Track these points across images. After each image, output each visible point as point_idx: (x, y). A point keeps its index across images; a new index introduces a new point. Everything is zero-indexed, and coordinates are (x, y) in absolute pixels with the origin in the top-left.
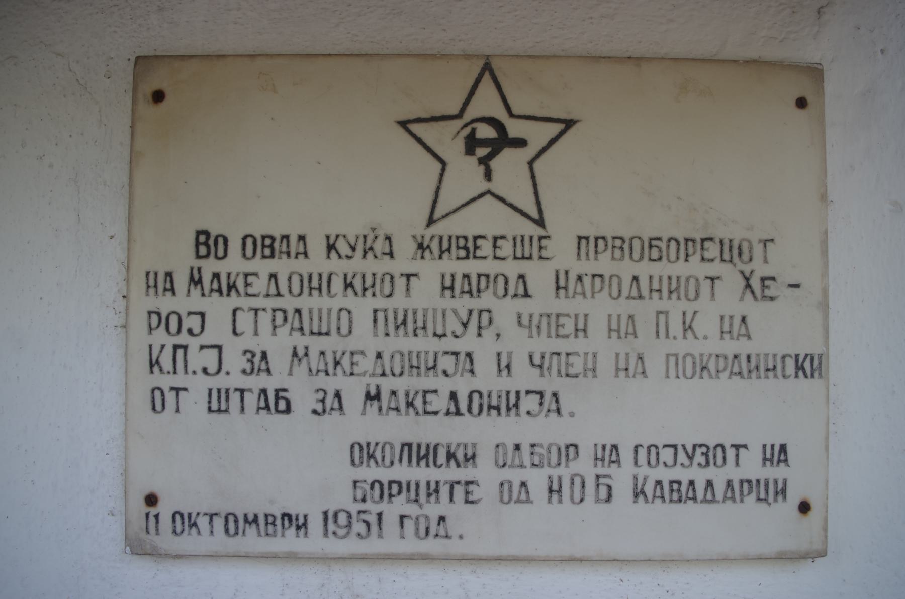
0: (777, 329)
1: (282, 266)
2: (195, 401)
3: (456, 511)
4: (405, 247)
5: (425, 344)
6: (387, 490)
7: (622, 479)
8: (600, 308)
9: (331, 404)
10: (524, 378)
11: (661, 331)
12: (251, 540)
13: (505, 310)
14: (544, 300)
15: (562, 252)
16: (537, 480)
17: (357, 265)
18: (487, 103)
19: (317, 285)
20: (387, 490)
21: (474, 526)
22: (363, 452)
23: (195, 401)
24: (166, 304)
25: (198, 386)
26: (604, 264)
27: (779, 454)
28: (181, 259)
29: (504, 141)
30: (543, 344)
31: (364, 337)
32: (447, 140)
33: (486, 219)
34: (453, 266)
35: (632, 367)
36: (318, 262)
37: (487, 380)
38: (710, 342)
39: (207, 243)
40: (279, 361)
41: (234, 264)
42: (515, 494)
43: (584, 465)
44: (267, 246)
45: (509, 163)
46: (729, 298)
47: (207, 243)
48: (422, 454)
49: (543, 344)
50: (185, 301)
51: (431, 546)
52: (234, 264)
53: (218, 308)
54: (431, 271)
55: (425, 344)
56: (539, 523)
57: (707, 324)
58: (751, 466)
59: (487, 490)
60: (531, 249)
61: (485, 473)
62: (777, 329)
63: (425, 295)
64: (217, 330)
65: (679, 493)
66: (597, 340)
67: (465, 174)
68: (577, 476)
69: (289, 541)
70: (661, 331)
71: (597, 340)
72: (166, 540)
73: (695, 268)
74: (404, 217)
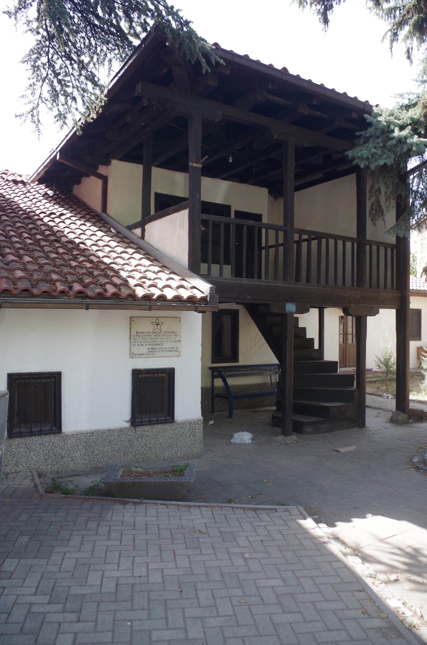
0: (177, 338)
1: (143, 334)
2: (136, 345)
3: (155, 353)
4: (151, 333)
5: (153, 340)
6: (150, 352)
7: (166, 350)
8: (165, 337)
9: (146, 345)
10: (160, 343)
11: (169, 339)
12: (141, 356)
13: (158, 337)
14: (161, 337)
15: (162, 332)
16: (161, 350)
17: (148, 334)
18: (157, 321)
19: (145, 336)
20: (150, 352)
21: (157, 354)
22: (149, 349)
23: (136, 345)
24: (134, 337)
25: (137, 344)
26: (165, 334)
27: (177, 348)
28: (135, 334)
29: (158, 324)
30: (161, 340)
31: (149, 340)
32: (154, 324)
33: (157, 330)
34: (155, 334)
35: (167, 342)
36: (145, 334)
37: (157, 343)
38: (173, 340)
39: (137, 332)
40: (143, 342)
41: (139, 334)
42: (159, 351)
43: (164, 349)
44: (142, 333)
45: (159, 326)
46: (174, 336)
47: (137, 332)
48: (153, 349)
49: (161, 340)
50: (136, 337)
51: (154, 356)
52: (139, 334)
53: (138, 338)
54: (153, 334)
55: (153, 340)
56: (161, 354)
57: (172, 338)
58: (175, 349)
59: (157, 351)
60: (160, 333)
61: (157, 350)
62: (177, 338)
63: (153, 336)
64: (138, 339)
65: (170, 351)
66: (165, 340)
67: (156, 326)
68: (164, 350)
69: (143, 356)
70: (169, 339)
71: (165, 340)
72: (134, 356)
73: (172, 334)
74: (151, 330)
